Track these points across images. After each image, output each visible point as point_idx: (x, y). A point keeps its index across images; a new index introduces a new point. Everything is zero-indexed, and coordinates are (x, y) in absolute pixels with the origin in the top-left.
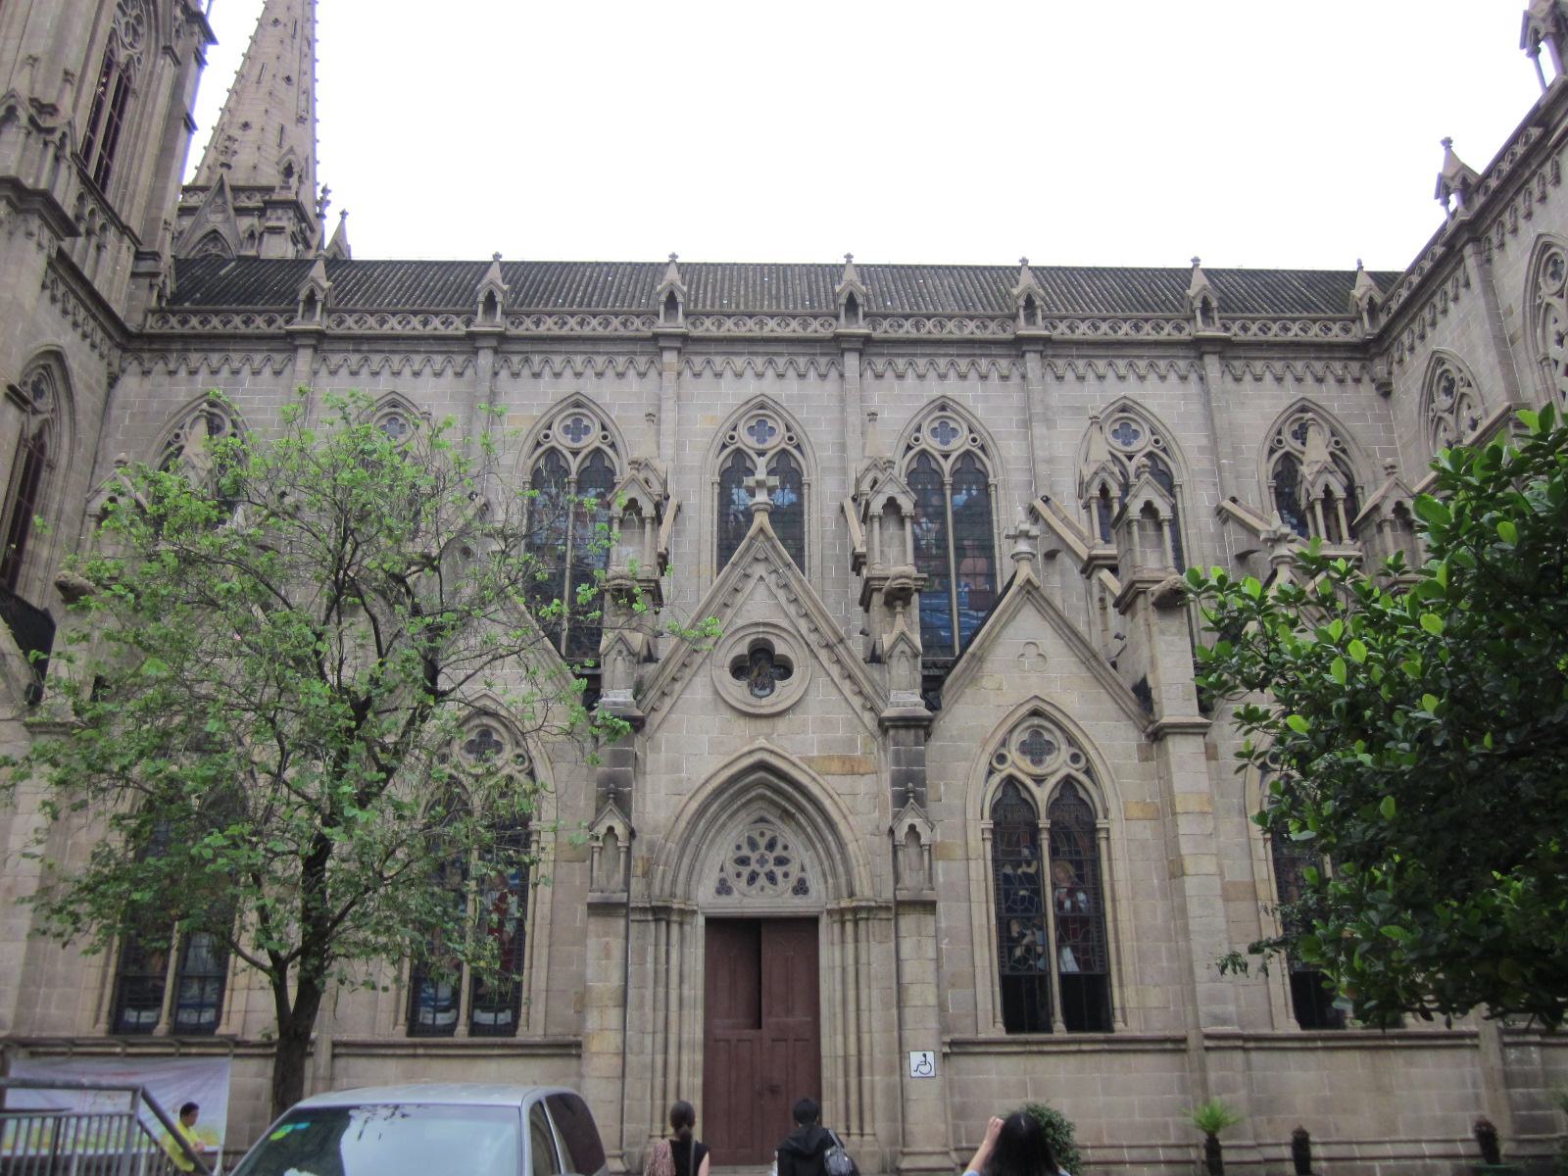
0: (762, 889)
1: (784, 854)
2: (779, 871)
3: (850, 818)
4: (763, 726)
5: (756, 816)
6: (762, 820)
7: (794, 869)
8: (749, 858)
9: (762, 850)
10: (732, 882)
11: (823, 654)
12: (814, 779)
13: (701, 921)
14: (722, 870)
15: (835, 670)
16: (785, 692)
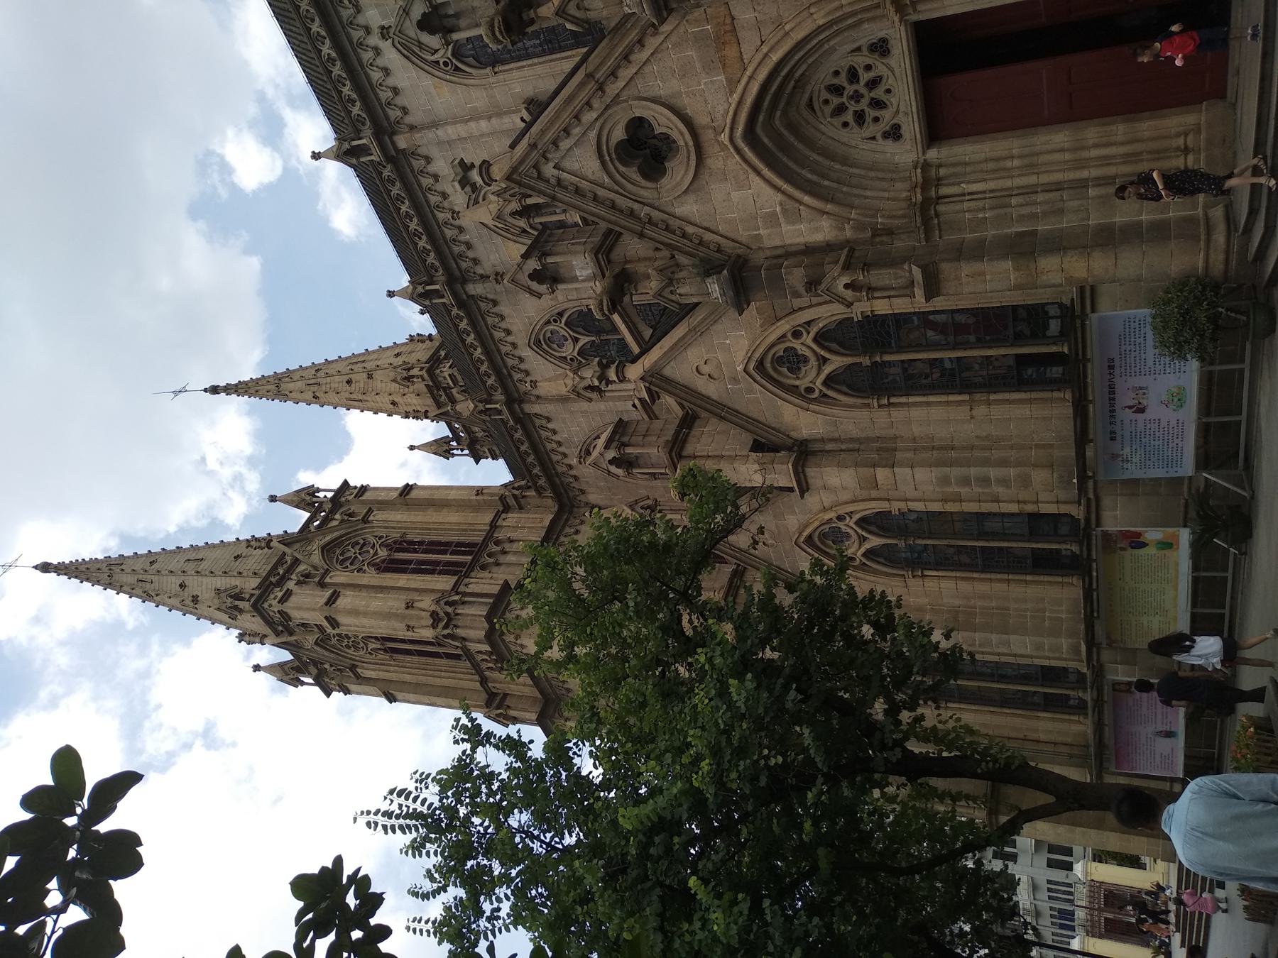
3: (787, 27)
4: (707, 137)
5: (806, 113)
6: (810, 105)
7: (860, 61)
8: (856, 112)
11: (613, 89)
12: (751, 78)
13: (932, 154)
14: (874, 138)
15: (625, 73)
16: (663, 121)
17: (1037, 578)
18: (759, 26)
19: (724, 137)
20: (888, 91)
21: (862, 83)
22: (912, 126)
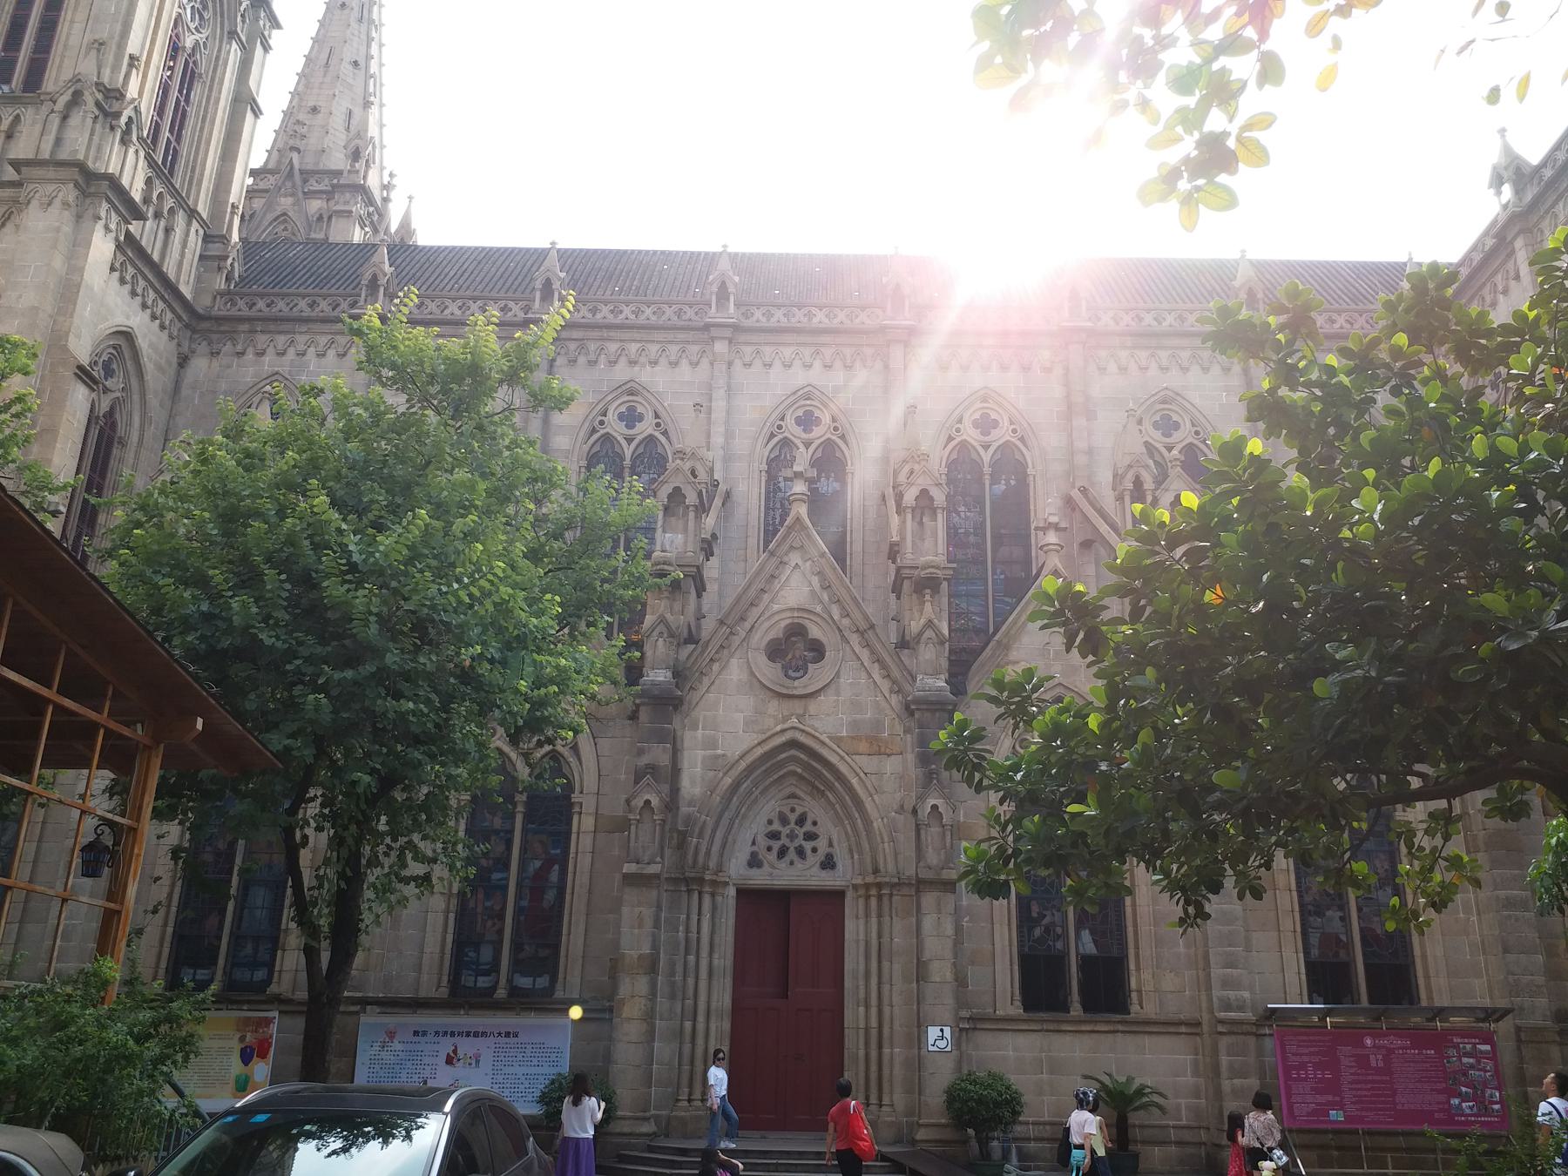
0: (792, 863)
1: (813, 829)
2: (808, 846)
3: (875, 797)
4: (797, 706)
5: (787, 791)
6: (793, 796)
7: (822, 844)
8: (780, 833)
9: (792, 825)
10: (763, 854)
11: (854, 639)
12: (842, 758)
13: (732, 891)
14: (754, 843)
15: (865, 655)
16: (817, 675)
17: (168, 938)
18: (879, 774)
19: (794, 721)
20: (792, 863)
21: (803, 843)
22: (760, 878)
